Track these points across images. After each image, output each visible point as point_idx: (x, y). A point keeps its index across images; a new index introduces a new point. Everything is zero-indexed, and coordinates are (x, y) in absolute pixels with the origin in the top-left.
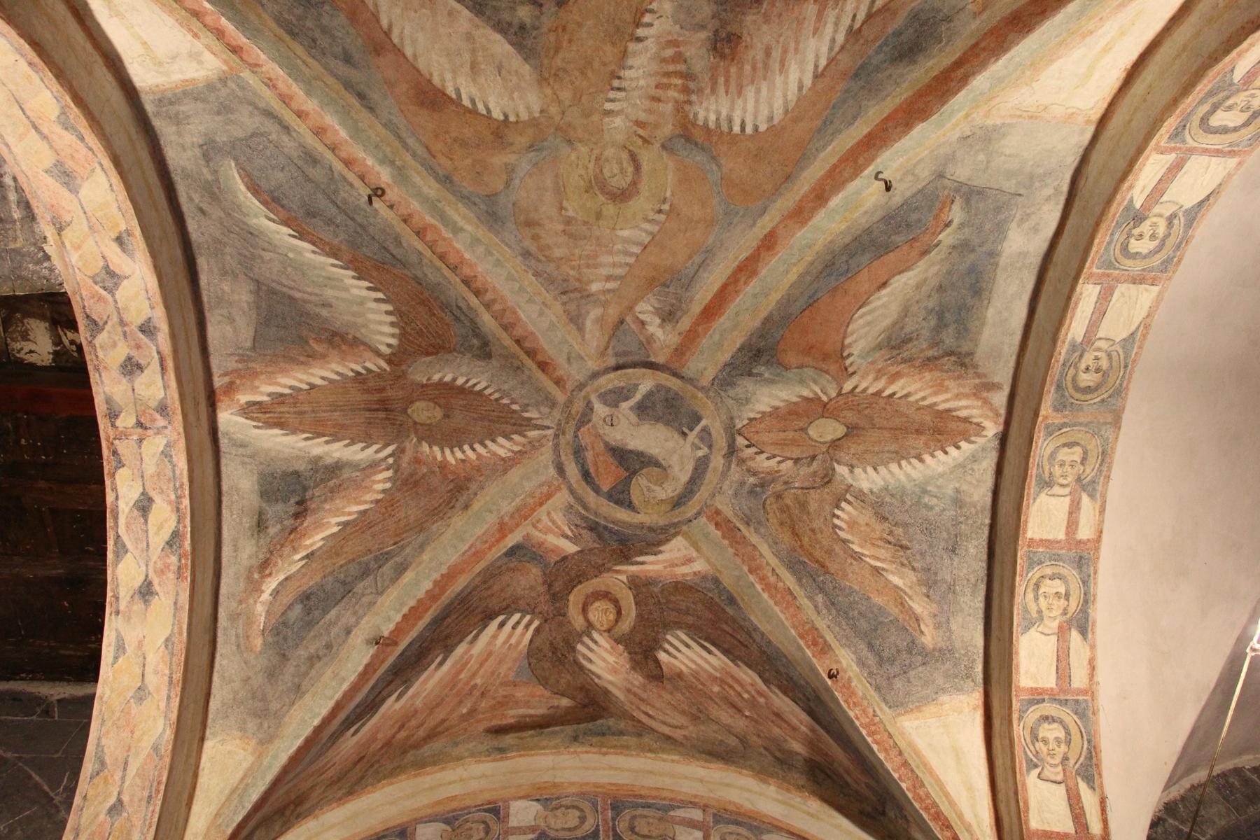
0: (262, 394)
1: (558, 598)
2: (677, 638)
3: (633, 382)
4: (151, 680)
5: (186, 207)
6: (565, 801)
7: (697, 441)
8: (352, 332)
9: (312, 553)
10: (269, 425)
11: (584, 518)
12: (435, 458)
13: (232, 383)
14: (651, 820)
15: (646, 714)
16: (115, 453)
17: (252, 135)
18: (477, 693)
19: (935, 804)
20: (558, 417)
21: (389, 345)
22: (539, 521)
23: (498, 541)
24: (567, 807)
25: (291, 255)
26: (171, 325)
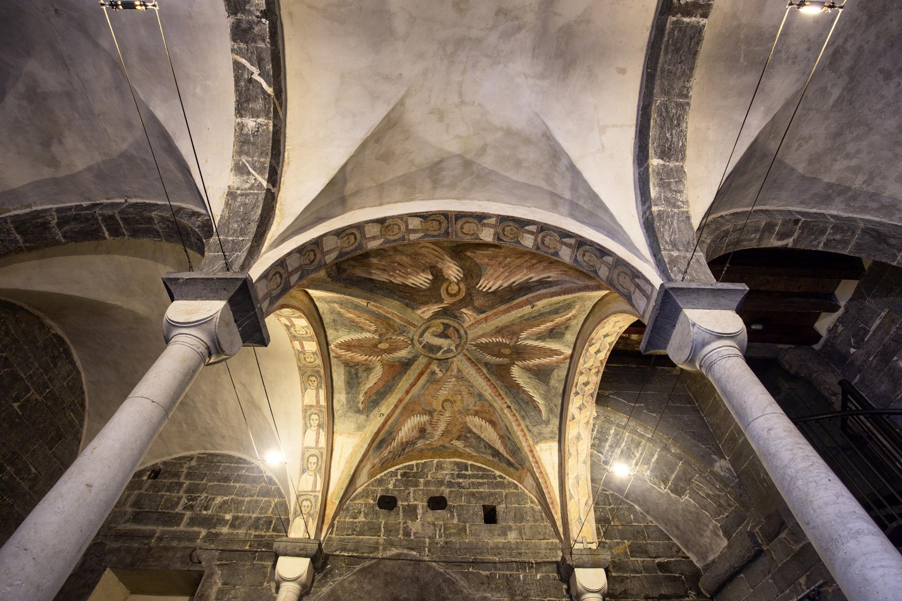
1: (469, 294)
2: (425, 286)
10: (556, 350)
11: (459, 320)
14: (432, 229)
15: (436, 251)
16: (602, 363)
17: (535, 426)
18: (503, 265)
24: (468, 234)
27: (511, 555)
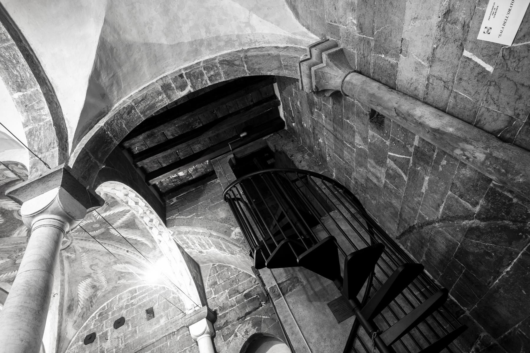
10: (124, 211)
27: (162, 334)
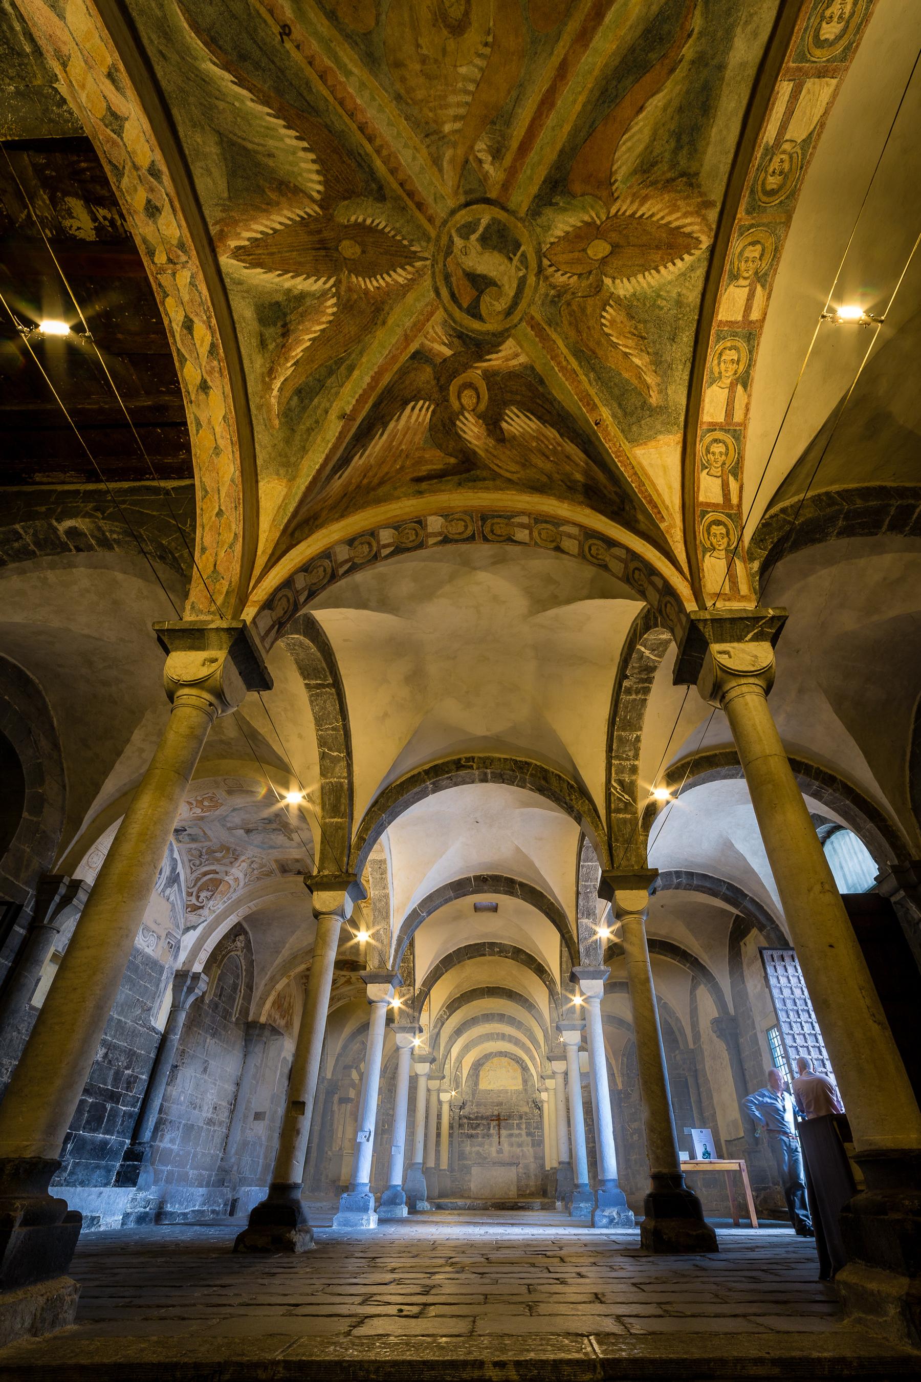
0: (243, 239)
1: (443, 388)
3: (477, 216)
4: (221, 443)
5: (151, 51)
6: (456, 516)
7: (518, 264)
8: (292, 180)
9: (297, 361)
11: (454, 329)
12: (360, 286)
13: (222, 231)
15: (498, 465)
16: (160, 285)
18: (404, 456)
19: (650, 495)
20: (432, 249)
21: (319, 192)
22: (428, 333)
23: (405, 348)
25: (237, 104)
26: (169, 169)
